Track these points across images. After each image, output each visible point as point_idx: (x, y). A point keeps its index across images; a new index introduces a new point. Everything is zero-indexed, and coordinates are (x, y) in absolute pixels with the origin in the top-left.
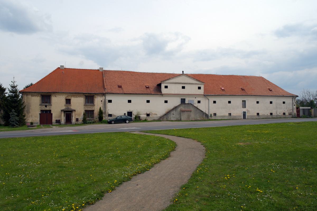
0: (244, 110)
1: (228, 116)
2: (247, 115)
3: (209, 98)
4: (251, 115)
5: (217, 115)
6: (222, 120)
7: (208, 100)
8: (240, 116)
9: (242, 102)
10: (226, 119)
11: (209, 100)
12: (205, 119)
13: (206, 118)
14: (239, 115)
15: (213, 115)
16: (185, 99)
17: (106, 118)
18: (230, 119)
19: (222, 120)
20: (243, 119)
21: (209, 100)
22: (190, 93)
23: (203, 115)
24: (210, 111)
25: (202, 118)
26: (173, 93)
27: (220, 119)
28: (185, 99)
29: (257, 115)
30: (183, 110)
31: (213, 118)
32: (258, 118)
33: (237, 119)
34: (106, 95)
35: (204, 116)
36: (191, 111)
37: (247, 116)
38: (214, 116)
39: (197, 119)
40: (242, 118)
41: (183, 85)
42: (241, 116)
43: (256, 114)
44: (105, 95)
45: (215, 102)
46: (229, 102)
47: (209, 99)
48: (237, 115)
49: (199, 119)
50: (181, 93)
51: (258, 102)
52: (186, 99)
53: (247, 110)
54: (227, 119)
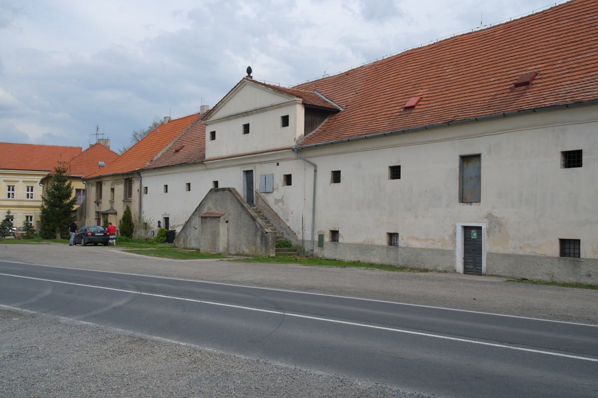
0: (471, 215)
1: (383, 247)
2: (487, 247)
3: (313, 160)
4: (510, 251)
5: (340, 240)
6: (357, 264)
7: (311, 171)
8: (443, 253)
9: (456, 164)
10: (371, 265)
11: (319, 169)
12: (261, 252)
13: (264, 249)
14: (438, 246)
15: (327, 239)
16: (252, 171)
17: (139, 233)
18: (393, 262)
19: (357, 264)
20: (466, 271)
21: (315, 171)
22: (260, 149)
23: (256, 235)
24: (318, 217)
25: (253, 248)
26: (225, 154)
27: (352, 258)
28: (252, 171)
29: (563, 253)
30: (212, 213)
31: (328, 252)
32: (572, 279)
33: (428, 266)
34: (142, 175)
35: (259, 240)
36: (219, 217)
37: (490, 254)
38: (332, 245)
39: (241, 252)
40: (459, 266)
41: (245, 121)
42: (452, 253)
43: (555, 250)
44: (140, 175)
45: (336, 177)
46: (395, 172)
47: (315, 166)
48: (429, 245)
49: (247, 251)
50: (241, 151)
51: (573, 159)
52: (254, 172)
53: (489, 216)
54: (376, 260)
